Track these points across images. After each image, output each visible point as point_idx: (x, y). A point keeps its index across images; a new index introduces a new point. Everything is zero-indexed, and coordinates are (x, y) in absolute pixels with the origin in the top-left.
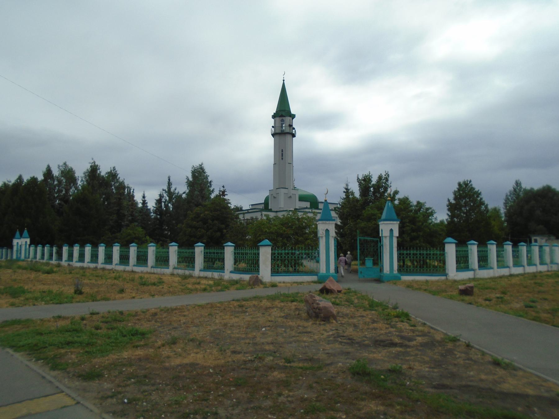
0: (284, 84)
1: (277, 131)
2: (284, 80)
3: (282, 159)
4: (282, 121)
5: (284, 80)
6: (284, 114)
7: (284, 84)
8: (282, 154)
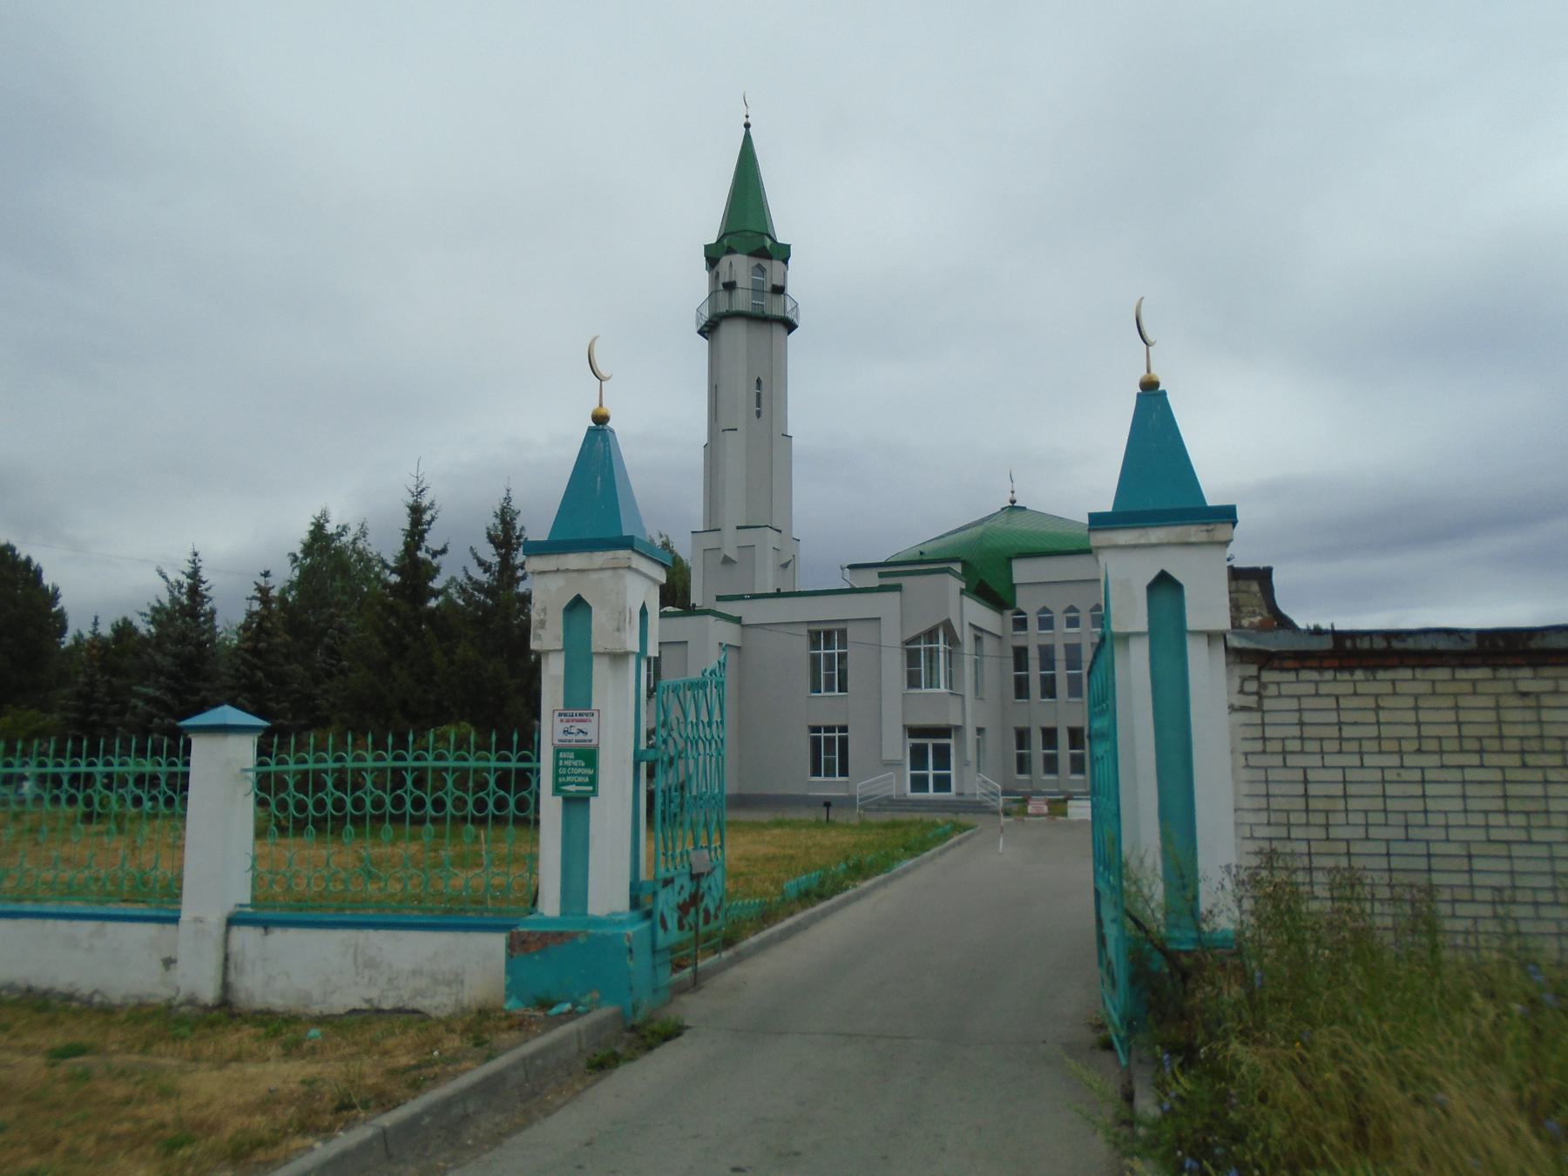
0: (747, 139)
2: (747, 126)
3: (759, 414)
4: (760, 269)
5: (747, 126)
7: (747, 139)
8: (759, 395)
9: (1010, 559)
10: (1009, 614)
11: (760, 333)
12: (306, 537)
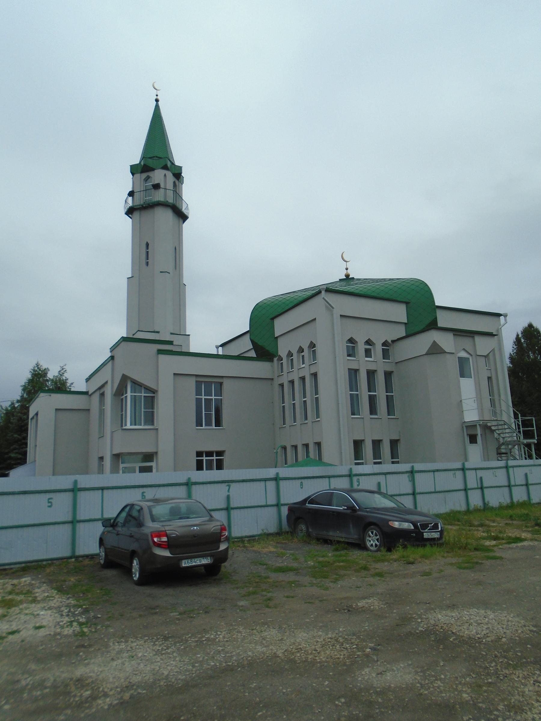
0: (157, 108)
1: (137, 203)
2: (157, 100)
3: (147, 264)
5: (157, 100)
6: (150, 163)
7: (157, 108)
8: (147, 253)
9: (273, 319)
10: (275, 359)
11: (147, 215)
12: (29, 376)
